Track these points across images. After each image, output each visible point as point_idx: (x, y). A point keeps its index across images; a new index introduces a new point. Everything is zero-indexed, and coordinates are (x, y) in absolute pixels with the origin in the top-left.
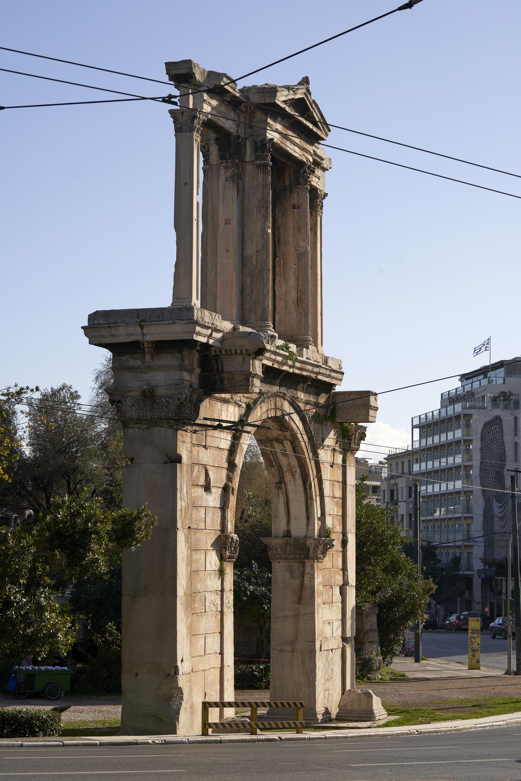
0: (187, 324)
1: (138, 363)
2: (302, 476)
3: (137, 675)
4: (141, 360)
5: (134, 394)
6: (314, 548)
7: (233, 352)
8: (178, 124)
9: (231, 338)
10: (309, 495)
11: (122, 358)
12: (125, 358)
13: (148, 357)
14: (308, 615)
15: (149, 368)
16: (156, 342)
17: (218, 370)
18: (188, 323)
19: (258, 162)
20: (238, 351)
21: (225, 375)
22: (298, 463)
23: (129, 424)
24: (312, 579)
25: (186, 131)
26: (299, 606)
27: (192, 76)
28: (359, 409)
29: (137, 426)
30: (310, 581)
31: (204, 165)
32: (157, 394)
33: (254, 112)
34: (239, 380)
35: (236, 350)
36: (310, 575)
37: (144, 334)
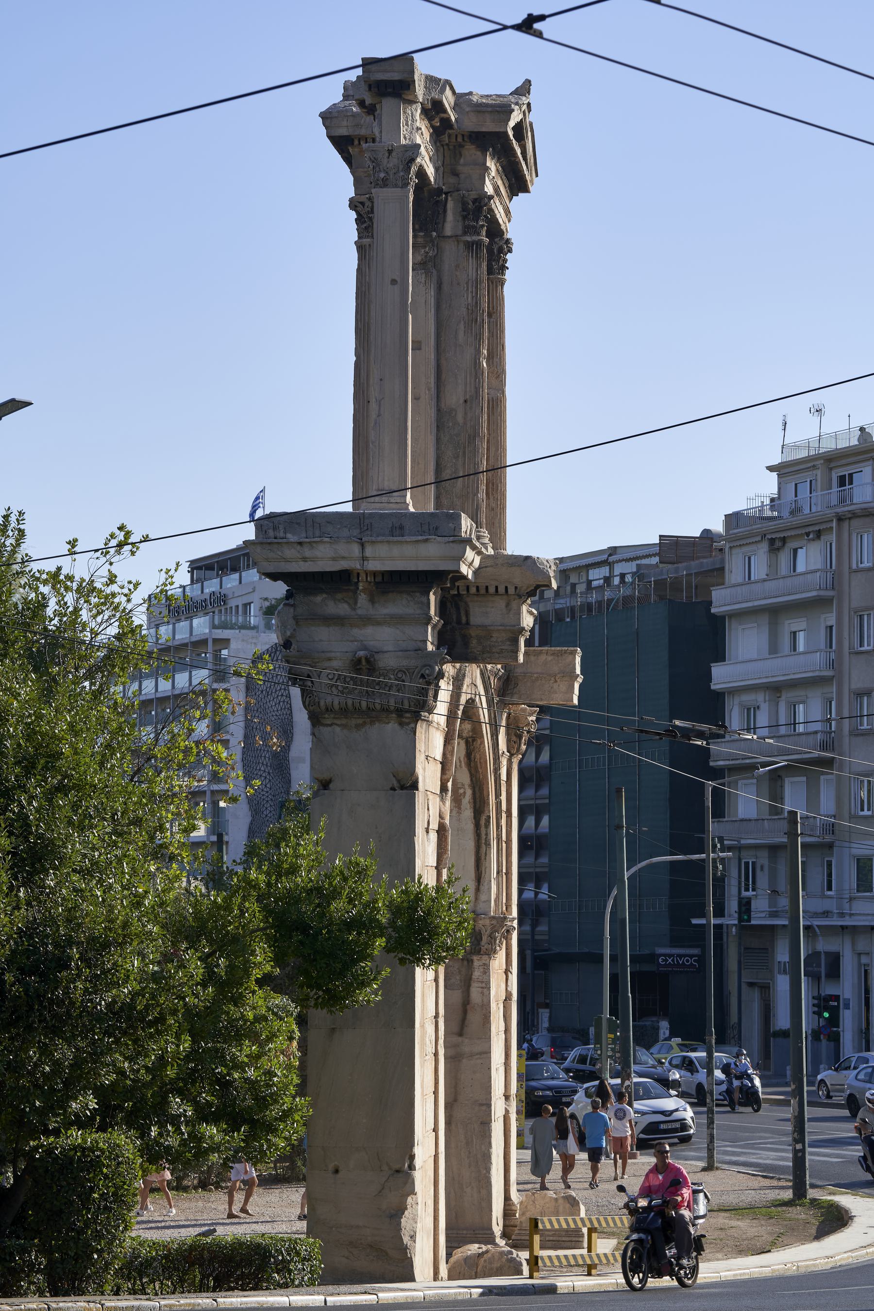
0: (451, 544)
1: (342, 609)
2: (475, 802)
3: (336, 1171)
4: (349, 604)
5: (335, 664)
6: (492, 933)
7: (492, 590)
8: (380, 171)
9: (492, 566)
10: (484, 837)
11: (312, 598)
12: (319, 599)
13: (363, 599)
14: (478, 1056)
15: (367, 621)
16: (383, 573)
17: (459, 622)
18: (452, 542)
19: (468, 238)
20: (501, 590)
21: (473, 632)
22: (471, 780)
23: (325, 718)
24: (485, 990)
25: (396, 186)
26: (460, 1039)
27: (409, 85)
28: (556, 681)
29: (338, 722)
30: (482, 993)
31: (359, 237)
32: (380, 666)
33: (461, 146)
34: (499, 640)
35: (497, 587)
36: (482, 982)
37: (364, 559)
